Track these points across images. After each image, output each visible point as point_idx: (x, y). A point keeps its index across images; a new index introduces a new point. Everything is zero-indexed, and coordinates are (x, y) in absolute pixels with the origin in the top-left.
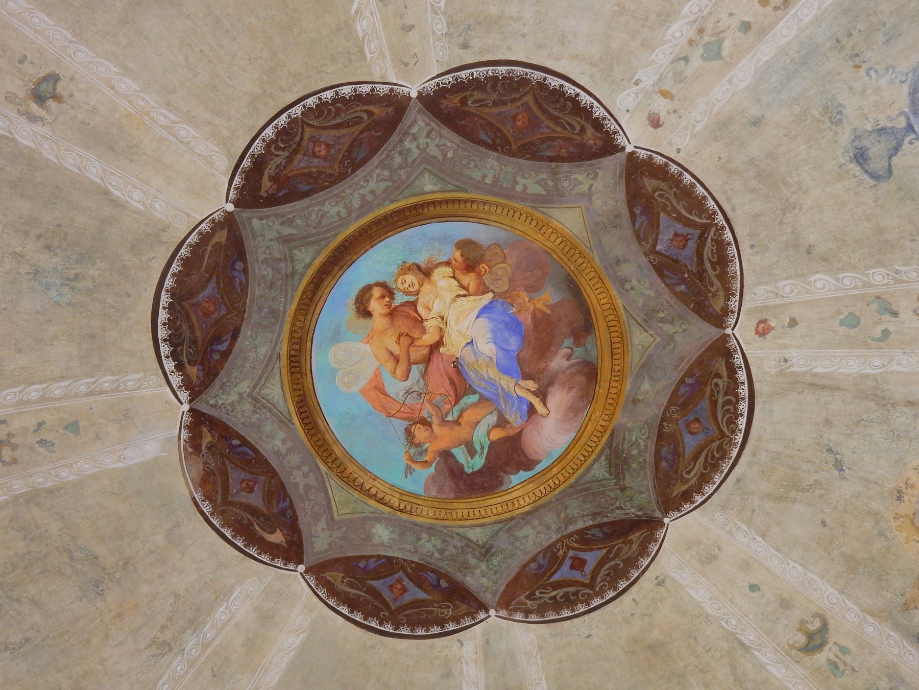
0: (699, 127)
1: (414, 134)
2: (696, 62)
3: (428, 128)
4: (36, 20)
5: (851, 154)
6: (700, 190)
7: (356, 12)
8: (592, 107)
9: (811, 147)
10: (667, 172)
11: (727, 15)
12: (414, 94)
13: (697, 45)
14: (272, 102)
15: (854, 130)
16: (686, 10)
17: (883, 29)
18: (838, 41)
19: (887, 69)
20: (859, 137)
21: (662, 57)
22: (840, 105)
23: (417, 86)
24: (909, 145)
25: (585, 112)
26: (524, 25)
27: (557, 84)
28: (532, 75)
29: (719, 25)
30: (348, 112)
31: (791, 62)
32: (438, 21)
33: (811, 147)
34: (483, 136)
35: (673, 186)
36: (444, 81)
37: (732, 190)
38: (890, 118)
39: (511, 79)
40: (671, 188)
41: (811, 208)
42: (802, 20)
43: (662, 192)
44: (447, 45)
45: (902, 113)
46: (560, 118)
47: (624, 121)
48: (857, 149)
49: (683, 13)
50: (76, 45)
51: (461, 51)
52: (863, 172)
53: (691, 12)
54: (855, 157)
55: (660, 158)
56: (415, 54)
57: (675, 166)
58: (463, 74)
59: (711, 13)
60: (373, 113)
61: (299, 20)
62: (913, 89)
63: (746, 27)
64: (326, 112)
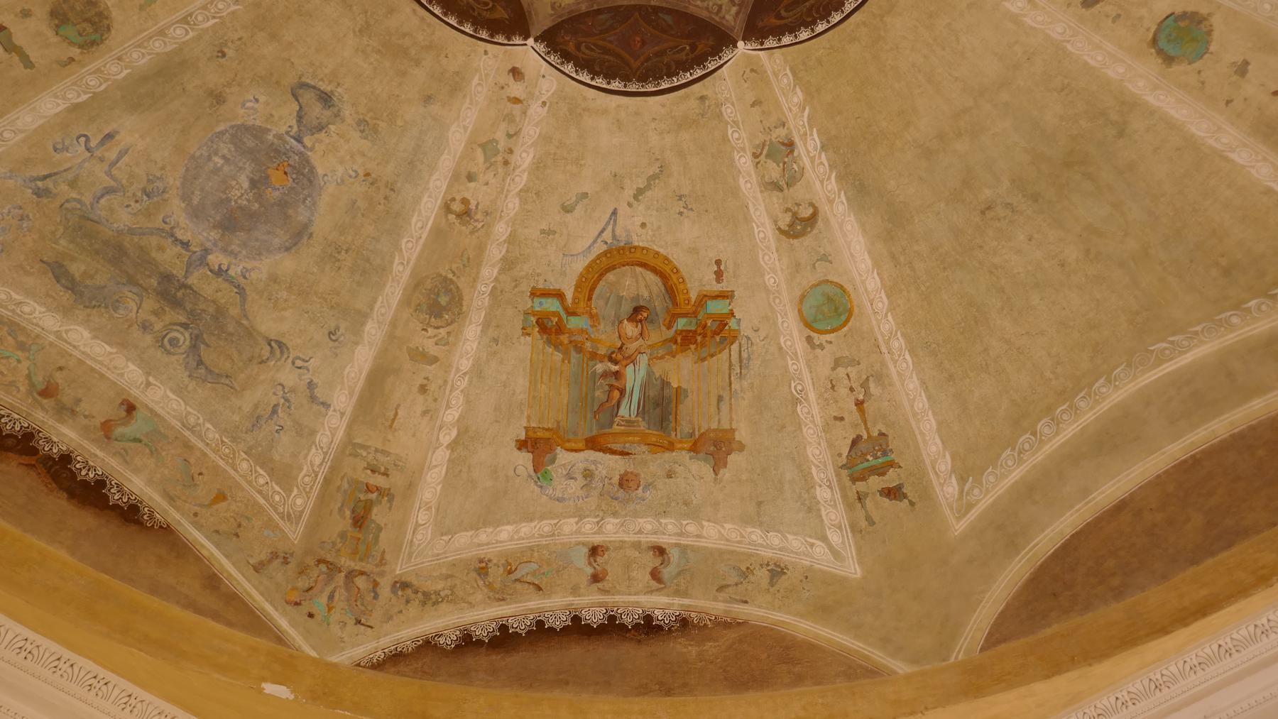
0: (476, 81)
1: (734, 6)
2: (500, 135)
3: (721, 15)
4: (1100, 58)
5: (335, 99)
6: (453, 21)
7: (804, 109)
8: (576, 71)
9: (372, 92)
10: (488, 29)
11: (490, 182)
12: (740, 44)
13: (505, 151)
14: (874, 10)
15: (343, 121)
16: (525, 176)
17: (362, 211)
18: (392, 190)
19: (343, 181)
20: (336, 116)
21: (530, 132)
22: (366, 138)
23: (739, 53)
24: (291, 125)
25: (581, 65)
26: (655, 129)
27: (614, 84)
28: (637, 87)
29: (493, 173)
30: (800, 14)
31: (422, 161)
32: (731, 115)
33: (372, 92)
34: (669, 19)
35: (479, 18)
36: (715, 62)
37: (424, 30)
38: (321, 141)
39: (656, 79)
40: (479, 14)
41: (345, 36)
42: (429, 197)
43: (486, 8)
44: (719, 96)
45: (312, 149)
46: (601, 53)
47: (544, 66)
48: (333, 105)
49: (526, 174)
50: (1063, 39)
51: (705, 94)
52: (317, 86)
53: (520, 176)
54: (330, 97)
55: (500, 41)
56: (746, 82)
57: (483, 37)
58: (699, 73)
59: (503, 180)
60: (775, 18)
61: (854, 92)
62: (313, 173)
63: (471, 178)
64: (821, 9)
